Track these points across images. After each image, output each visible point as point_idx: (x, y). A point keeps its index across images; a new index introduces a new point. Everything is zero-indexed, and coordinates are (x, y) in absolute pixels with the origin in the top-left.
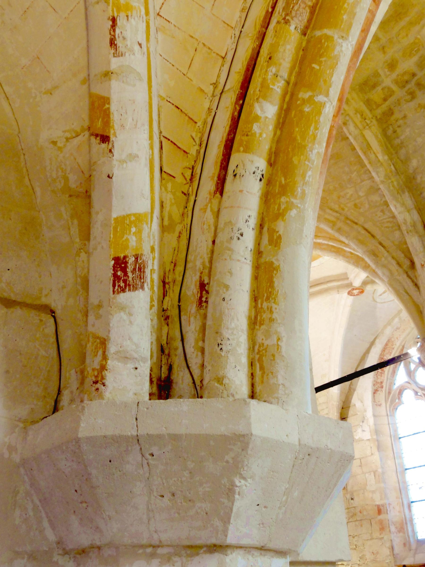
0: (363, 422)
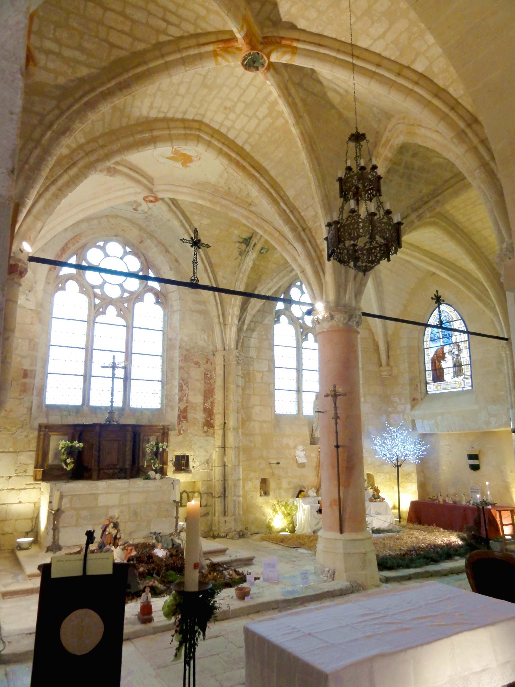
0: (30, 291)
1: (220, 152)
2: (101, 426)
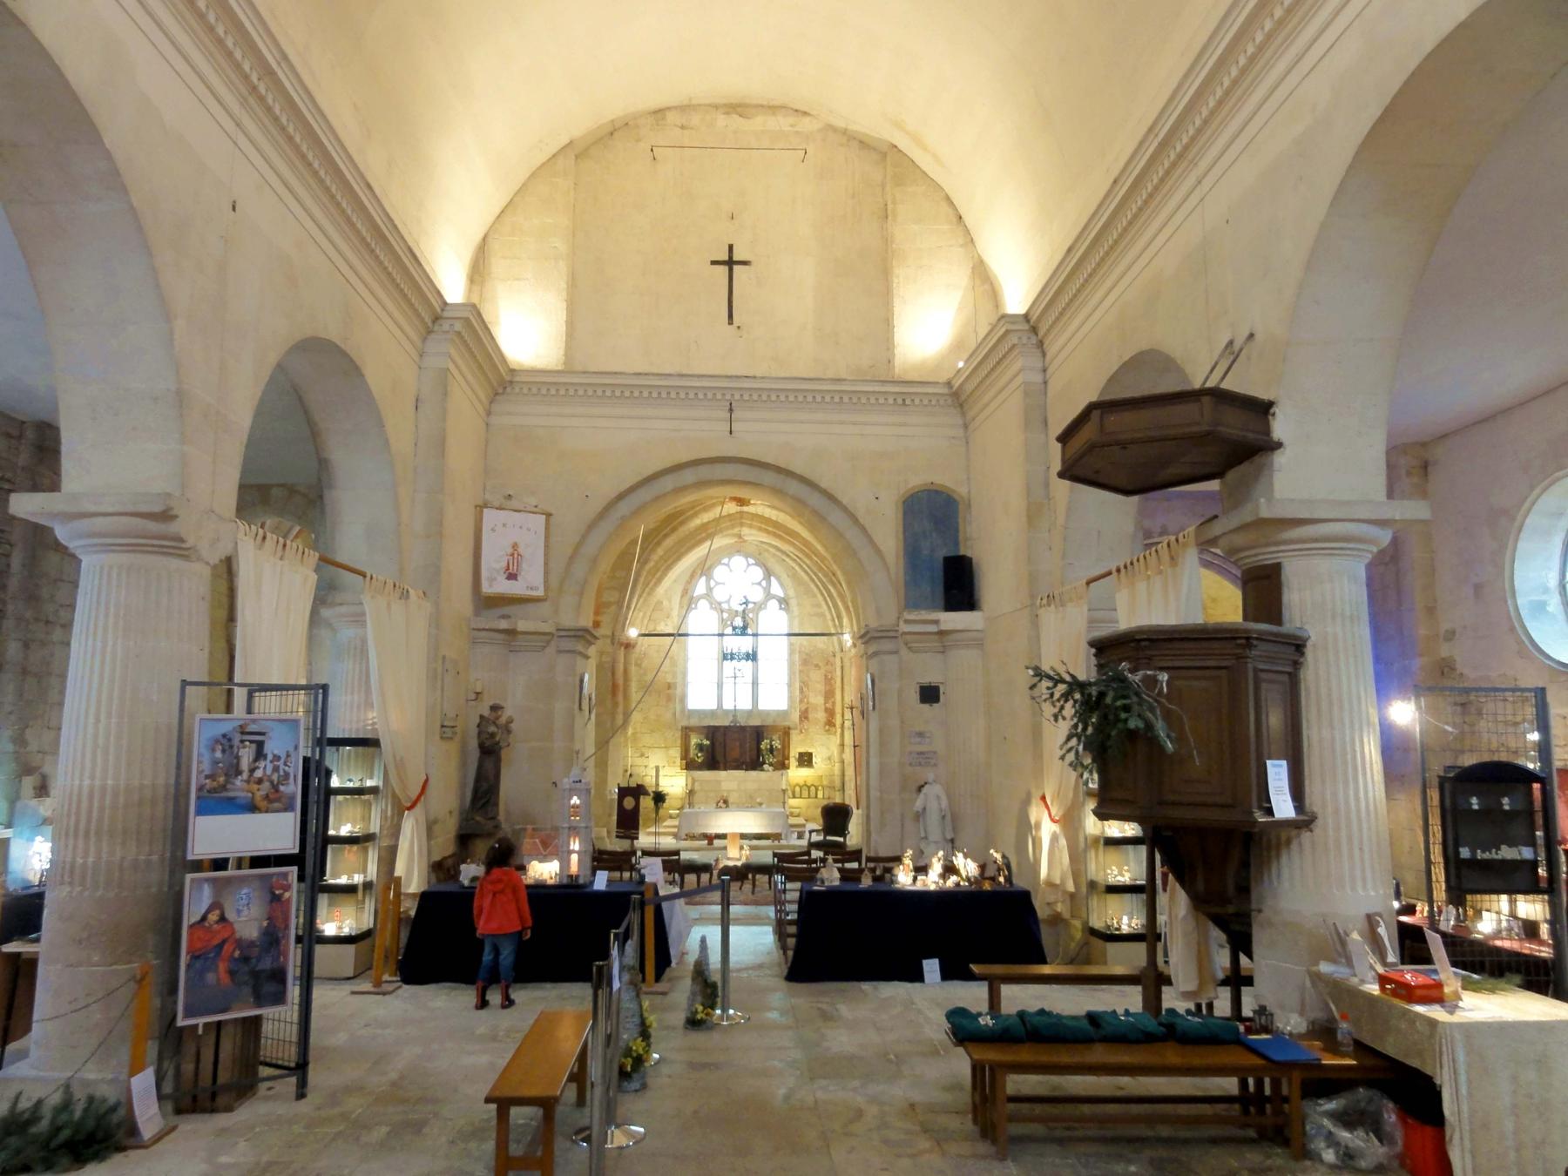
1: (760, 529)
2: (726, 728)
